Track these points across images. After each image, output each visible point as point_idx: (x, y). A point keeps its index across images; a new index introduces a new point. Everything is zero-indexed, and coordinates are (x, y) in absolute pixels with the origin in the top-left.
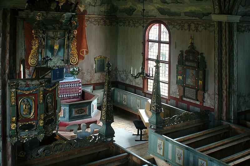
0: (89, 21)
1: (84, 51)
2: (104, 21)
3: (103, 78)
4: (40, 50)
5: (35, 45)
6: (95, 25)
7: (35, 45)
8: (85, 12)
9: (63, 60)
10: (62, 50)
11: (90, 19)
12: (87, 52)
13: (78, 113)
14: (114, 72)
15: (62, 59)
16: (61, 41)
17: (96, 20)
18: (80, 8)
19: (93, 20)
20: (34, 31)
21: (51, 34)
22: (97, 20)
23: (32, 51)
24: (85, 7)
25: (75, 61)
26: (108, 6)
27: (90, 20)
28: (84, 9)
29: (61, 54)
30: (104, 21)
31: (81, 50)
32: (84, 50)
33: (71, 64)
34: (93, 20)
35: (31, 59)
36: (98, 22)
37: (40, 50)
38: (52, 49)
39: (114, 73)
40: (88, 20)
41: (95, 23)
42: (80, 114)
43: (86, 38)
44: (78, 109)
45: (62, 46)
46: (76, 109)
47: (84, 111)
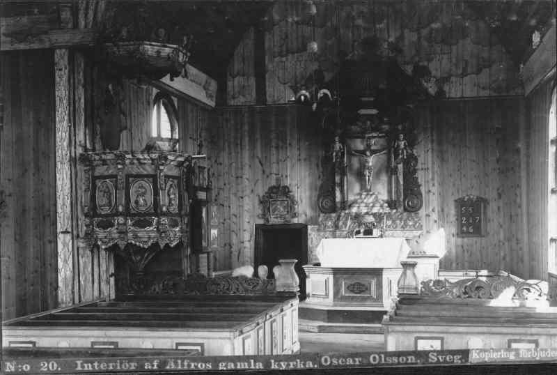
13: (352, 291)
21: (359, 144)
47: (367, 289)
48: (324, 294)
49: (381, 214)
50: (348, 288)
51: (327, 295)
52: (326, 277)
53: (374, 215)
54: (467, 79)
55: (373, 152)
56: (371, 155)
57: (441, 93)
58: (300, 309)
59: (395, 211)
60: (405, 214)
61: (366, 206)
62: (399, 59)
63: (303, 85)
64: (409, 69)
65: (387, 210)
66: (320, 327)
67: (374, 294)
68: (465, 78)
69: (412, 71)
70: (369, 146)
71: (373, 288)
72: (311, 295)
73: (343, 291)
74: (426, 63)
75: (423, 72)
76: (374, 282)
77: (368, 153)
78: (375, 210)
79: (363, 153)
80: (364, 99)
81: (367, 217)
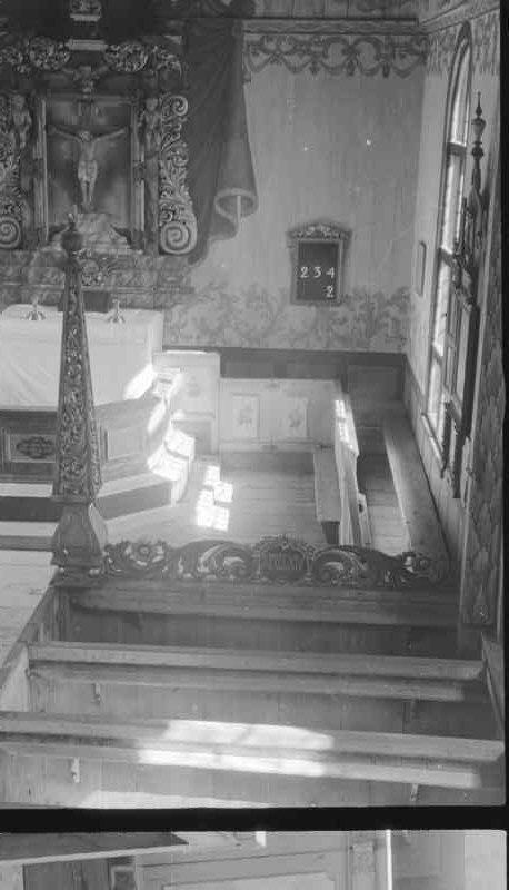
0: (265, 51)
1: (235, 197)
2: (344, 52)
4: (25, 184)
6: (294, 70)
9: (124, 233)
10: (119, 186)
12: (250, 204)
13: (28, 454)
14: (393, 311)
15: (122, 225)
16: (113, 145)
17: (302, 43)
19: (285, 47)
21: (66, 110)
22: (309, 44)
25: (172, 244)
27: (271, 46)
29: (113, 203)
30: (344, 52)
31: (221, 195)
32: (233, 192)
33: (162, 252)
34: (285, 47)
36: (314, 54)
37: (25, 184)
38: (66, 174)
40: (260, 46)
41: (294, 60)
42: (35, 458)
43: (244, 134)
44: (30, 436)
45: (116, 169)
46: (18, 437)
50: (18, 446)
59: (140, 252)
65: (125, 250)
78: (101, 249)
80: (77, 18)
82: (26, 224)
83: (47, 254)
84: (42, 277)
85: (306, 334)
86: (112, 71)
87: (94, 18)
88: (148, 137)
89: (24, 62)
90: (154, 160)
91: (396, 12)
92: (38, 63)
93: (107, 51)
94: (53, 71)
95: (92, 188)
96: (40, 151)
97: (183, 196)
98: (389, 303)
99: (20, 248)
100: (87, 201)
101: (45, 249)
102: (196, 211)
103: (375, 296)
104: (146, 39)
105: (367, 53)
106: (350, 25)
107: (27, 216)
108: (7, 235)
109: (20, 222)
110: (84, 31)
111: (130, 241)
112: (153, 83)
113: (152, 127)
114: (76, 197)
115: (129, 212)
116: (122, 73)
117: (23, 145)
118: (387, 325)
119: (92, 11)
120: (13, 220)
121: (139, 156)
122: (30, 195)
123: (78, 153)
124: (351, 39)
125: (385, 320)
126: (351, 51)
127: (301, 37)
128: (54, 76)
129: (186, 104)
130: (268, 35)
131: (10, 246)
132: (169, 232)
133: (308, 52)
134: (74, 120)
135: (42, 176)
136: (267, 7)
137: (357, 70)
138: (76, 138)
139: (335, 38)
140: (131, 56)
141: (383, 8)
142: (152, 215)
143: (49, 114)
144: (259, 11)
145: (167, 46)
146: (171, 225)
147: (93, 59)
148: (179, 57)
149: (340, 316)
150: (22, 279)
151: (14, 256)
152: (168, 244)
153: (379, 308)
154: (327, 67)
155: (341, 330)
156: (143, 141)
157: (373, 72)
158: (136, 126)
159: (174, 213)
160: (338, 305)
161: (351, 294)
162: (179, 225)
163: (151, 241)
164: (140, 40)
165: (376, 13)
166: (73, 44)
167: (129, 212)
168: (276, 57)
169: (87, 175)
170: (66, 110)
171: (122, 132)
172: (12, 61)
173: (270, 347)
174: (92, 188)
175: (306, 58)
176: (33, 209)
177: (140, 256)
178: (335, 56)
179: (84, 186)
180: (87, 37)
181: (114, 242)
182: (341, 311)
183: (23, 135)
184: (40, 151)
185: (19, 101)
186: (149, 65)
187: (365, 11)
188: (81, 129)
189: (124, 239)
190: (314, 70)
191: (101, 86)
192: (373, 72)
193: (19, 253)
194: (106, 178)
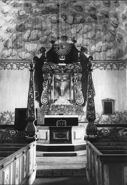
0: (95, 66)
2: (110, 66)
3: (111, 120)
4: (49, 91)
5: (45, 87)
6: (101, 69)
7: (45, 87)
8: (91, 57)
9: (70, 100)
10: (68, 91)
11: (96, 64)
13: (58, 137)
15: (69, 99)
17: (102, 65)
18: (85, 54)
19: (99, 65)
20: (44, 75)
21: (58, 77)
23: (43, 91)
24: (90, 53)
25: (80, 103)
26: (114, 51)
27: (96, 65)
28: (89, 56)
29: (67, 95)
30: (110, 66)
33: (77, 104)
35: (43, 98)
36: (105, 67)
38: (58, 89)
39: (123, 116)
40: (94, 65)
41: (101, 68)
44: (59, 133)
45: (68, 87)
46: (57, 133)
47: (64, 136)
48: (45, 138)
49: (67, 105)
51: (47, 139)
52: (46, 131)
53: (64, 106)
54: (101, 53)
55: (64, 80)
56: (63, 82)
57: (91, 57)
58: (37, 146)
59: (72, 104)
60: (77, 106)
61: (61, 102)
62: (76, 44)
63: (37, 53)
64: (79, 49)
66: (44, 154)
67: (68, 138)
68: (101, 53)
69: (81, 49)
70: (62, 78)
71: (68, 135)
72: (39, 139)
73: (54, 138)
74: (86, 47)
75: (84, 49)
76: (68, 133)
77: (62, 81)
78: (64, 104)
79: (60, 80)
80: (60, 59)
81: (61, 106)
82: (49, 99)
83: (53, 105)
84: (53, 109)
85: (107, 121)
86: (67, 69)
87: (64, 59)
88: (75, 80)
89: (50, 68)
90: (75, 86)
91: (119, 59)
92: (53, 68)
93: (66, 65)
94: (55, 69)
95: (63, 91)
96: (53, 84)
97: (81, 92)
98: (123, 114)
99: (48, 104)
100: (62, 94)
101: (53, 104)
102: (83, 95)
103: (120, 112)
104: (74, 63)
105: (115, 66)
106: (111, 62)
107: (49, 97)
108: (44, 102)
109: (48, 99)
110: (62, 62)
111: (70, 102)
112: (75, 71)
113: (75, 79)
114: (60, 94)
115: (70, 97)
116: (69, 69)
117: (50, 83)
118: (123, 118)
119: (63, 58)
120: (47, 99)
121: (72, 84)
122: (50, 93)
123: (61, 84)
124: (111, 64)
125: (123, 118)
126: (111, 66)
127: (102, 64)
128: (56, 70)
129: (81, 75)
130: (96, 63)
131: (46, 104)
132: (78, 101)
133: (103, 66)
134: (59, 78)
135: (53, 89)
136: (95, 58)
137: (113, 69)
138: (61, 82)
139: (108, 63)
140: (70, 66)
141: (117, 58)
142: (75, 97)
143: (55, 78)
144: (94, 59)
145: (78, 64)
146: (79, 99)
147: (63, 66)
148: (80, 66)
149: (113, 117)
150: (48, 110)
151: (46, 106)
152: (78, 103)
153: (121, 115)
154: (107, 69)
155: (114, 120)
156: (73, 82)
157: (116, 69)
158: (71, 79)
159: (79, 96)
160: (113, 115)
161: (115, 112)
162: (80, 99)
163: (75, 102)
164: (72, 63)
165: (115, 59)
166: (60, 64)
167: (70, 97)
168: (97, 67)
169: (62, 88)
170: (58, 77)
171: (69, 80)
172: (48, 67)
173: (100, 124)
174: (63, 91)
175: (103, 67)
176: (51, 96)
177: (73, 105)
178: (109, 67)
179: (61, 91)
180: (62, 63)
181: (67, 102)
182: (113, 116)
183: (50, 81)
184: (53, 84)
185: (49, 74)
186: (74, 68)
187: (113, 59)
188: (61, 80)
189: (69, 102)
190: (105, 69)
191: (65, 72)
192: (116, 69)
193: (48, 106)
194: (66, 90)
